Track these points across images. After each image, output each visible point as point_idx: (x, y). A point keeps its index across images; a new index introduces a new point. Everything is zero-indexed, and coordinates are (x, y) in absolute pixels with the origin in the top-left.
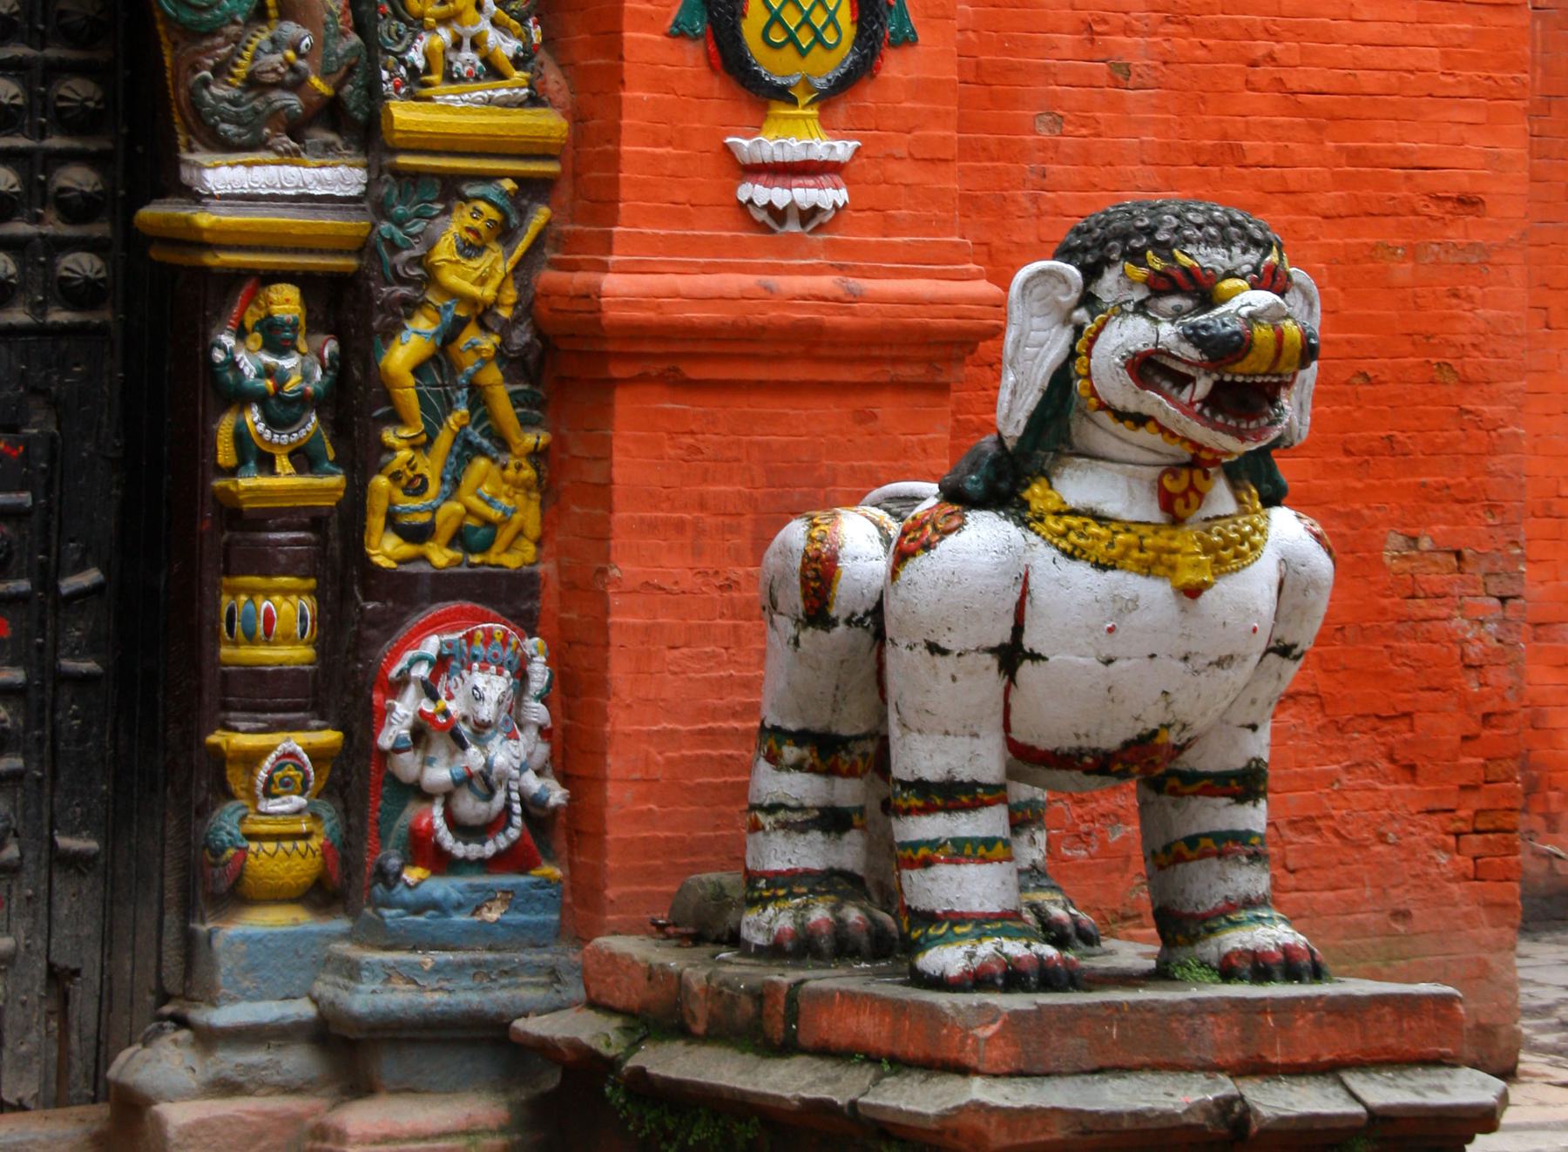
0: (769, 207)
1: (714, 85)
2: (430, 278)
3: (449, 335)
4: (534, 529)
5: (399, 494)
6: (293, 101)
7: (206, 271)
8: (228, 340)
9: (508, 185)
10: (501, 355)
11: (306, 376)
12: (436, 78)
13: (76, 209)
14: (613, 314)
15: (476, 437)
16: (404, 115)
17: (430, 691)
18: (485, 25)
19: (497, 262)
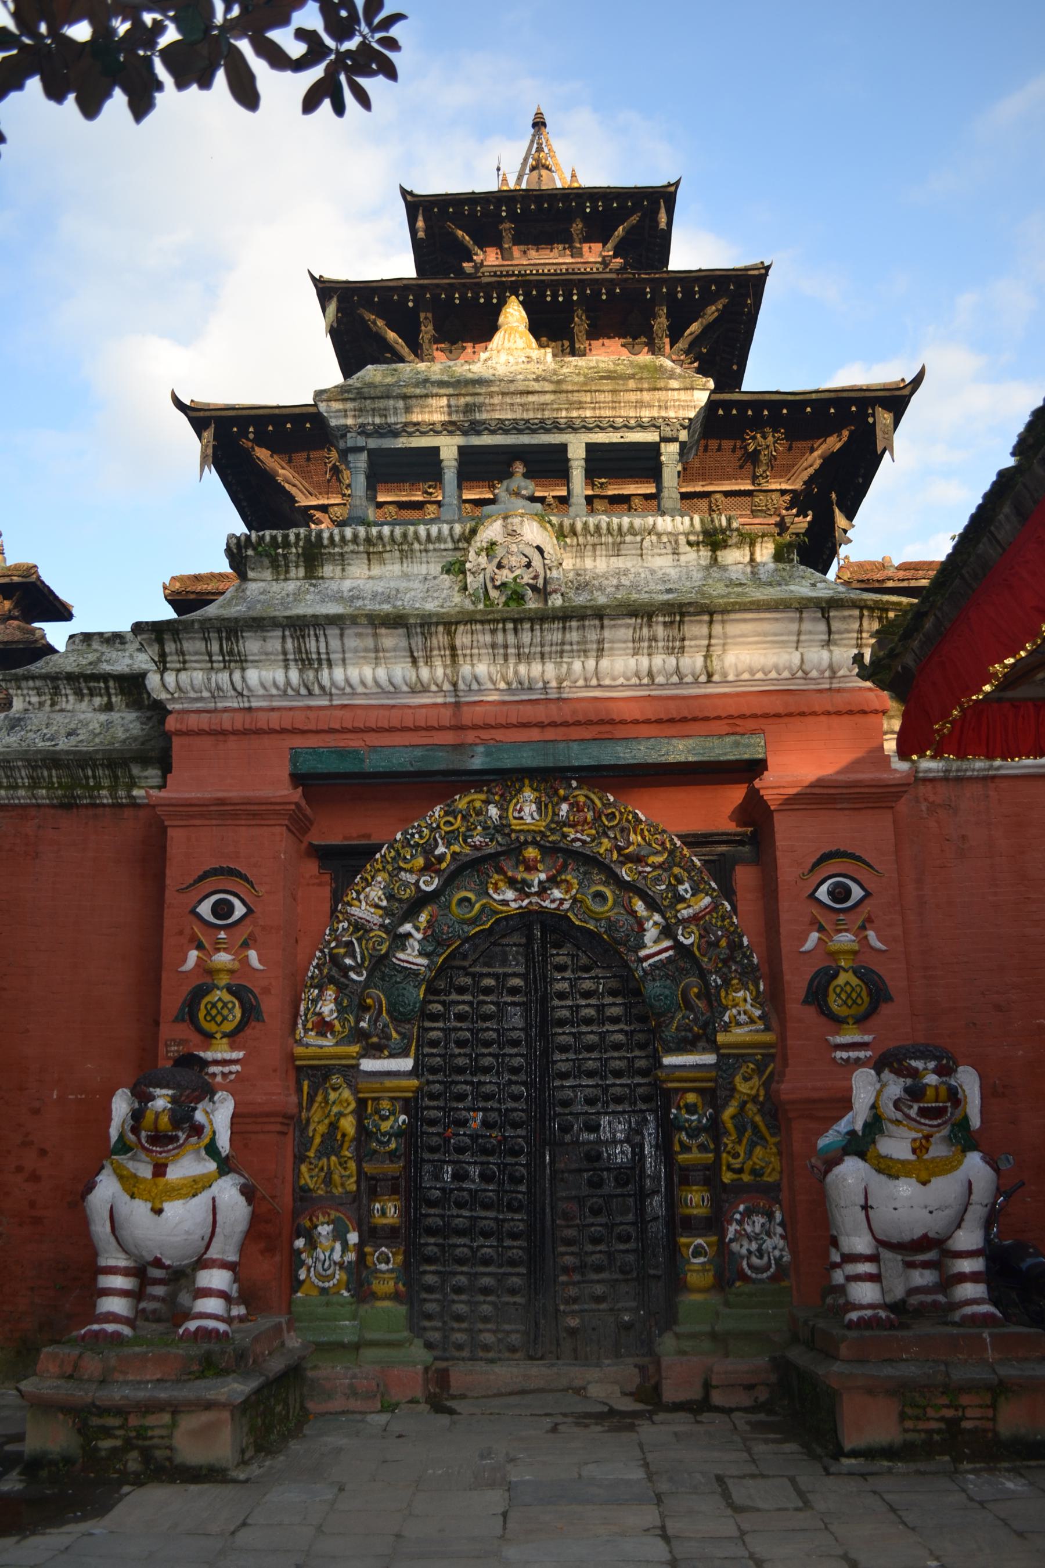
0: (841, 1058)
1: (823, 1020)
2: (734, 1089)
3: (743, 1105)
4: (779, 1169)
5: (730, 1159)
6: (689, 1035)
8: (674, 1111)
9: (759, 1057)
10: (759, 1110)
11: (699, 1121)
13: (644, 1073)
14: (783, 1097)
15: (755, 1139)
16: (721, 1038)
17: (740, 1223)
18: (748, 1007)
19: (755, 1081)
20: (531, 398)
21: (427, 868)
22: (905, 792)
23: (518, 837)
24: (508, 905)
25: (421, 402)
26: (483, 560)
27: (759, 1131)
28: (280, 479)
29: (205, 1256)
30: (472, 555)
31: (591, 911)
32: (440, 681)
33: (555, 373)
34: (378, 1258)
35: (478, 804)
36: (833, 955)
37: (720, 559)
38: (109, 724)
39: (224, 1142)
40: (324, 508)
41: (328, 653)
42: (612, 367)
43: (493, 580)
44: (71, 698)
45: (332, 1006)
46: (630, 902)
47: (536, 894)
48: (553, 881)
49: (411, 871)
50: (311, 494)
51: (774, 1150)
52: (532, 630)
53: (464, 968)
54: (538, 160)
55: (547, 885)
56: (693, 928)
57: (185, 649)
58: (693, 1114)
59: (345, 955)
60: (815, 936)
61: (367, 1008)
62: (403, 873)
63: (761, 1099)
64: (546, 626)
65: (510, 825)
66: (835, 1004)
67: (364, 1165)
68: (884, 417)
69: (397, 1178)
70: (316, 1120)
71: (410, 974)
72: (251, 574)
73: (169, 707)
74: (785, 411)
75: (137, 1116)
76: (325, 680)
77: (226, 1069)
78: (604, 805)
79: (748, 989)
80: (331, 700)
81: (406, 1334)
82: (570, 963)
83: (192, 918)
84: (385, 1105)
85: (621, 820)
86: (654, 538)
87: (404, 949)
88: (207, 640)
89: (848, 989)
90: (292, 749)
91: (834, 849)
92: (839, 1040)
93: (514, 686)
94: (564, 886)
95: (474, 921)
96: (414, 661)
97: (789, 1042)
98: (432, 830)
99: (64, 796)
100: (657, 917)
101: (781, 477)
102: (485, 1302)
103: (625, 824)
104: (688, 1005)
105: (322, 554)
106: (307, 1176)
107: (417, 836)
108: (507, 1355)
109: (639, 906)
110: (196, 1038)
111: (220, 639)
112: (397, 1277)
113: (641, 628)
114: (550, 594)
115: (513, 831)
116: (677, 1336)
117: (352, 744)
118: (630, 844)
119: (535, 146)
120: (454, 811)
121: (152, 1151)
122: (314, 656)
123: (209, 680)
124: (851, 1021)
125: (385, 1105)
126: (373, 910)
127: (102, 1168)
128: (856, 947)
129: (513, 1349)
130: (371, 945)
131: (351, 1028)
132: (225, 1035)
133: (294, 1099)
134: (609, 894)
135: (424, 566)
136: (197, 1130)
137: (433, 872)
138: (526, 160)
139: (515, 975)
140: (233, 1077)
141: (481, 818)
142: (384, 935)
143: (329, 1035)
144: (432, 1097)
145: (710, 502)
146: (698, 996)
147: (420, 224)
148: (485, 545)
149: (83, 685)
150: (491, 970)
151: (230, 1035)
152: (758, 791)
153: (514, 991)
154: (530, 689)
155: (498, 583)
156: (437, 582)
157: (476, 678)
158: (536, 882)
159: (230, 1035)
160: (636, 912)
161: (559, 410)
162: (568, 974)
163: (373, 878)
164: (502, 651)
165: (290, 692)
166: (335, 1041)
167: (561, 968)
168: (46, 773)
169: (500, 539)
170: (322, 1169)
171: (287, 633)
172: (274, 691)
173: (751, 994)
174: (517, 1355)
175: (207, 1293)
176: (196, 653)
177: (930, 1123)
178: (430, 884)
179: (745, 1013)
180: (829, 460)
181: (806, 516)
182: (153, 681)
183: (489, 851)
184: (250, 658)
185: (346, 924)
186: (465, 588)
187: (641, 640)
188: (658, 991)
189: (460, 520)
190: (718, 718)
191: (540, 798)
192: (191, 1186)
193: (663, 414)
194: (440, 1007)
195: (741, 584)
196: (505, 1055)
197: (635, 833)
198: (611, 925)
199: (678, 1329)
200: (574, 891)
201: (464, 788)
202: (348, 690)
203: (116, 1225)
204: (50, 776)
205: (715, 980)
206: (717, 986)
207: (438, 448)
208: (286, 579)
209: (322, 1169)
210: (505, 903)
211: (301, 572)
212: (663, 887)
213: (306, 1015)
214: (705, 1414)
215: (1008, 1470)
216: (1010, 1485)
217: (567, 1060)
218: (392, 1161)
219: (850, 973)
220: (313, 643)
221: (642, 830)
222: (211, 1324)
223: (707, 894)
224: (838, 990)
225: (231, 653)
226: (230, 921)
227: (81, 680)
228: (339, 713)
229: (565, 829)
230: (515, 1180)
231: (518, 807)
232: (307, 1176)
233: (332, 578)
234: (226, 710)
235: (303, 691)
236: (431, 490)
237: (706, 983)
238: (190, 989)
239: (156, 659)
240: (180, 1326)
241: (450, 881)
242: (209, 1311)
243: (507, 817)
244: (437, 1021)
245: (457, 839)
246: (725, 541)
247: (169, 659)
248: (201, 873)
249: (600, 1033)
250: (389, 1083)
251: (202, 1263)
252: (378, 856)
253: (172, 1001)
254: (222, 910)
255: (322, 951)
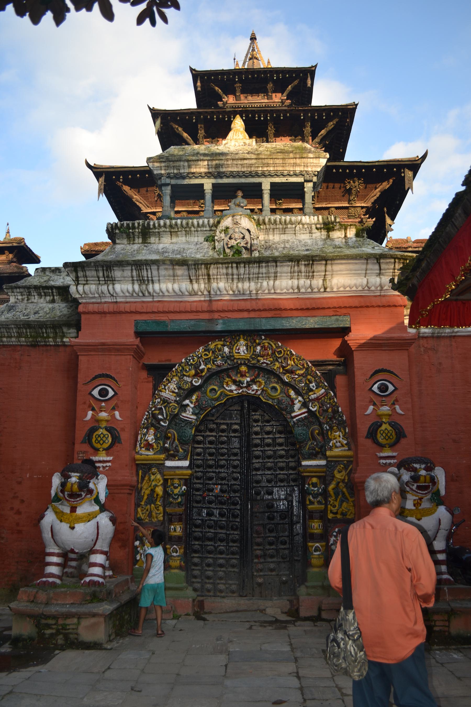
0: (383, 463)
1: (374, 445)
2: (334, 476)
4: (354, 513)
5: (332, 508)
6: (314, 451)
7: (301, 476)
8: (307, 486)
9: (346, 462)
10: (345, 486)
11: (318, 490)
12: (334, 447)
13: (294, 469)
14: (356, 480)
15: (343, 499)
16: (328, 453)
18: (341, 439)
19: (344, 473)
20: (245, 162)
21: (196, 375)
22: (414, 342)
23: (237, 362)
24: (233, 392)
25: (195, 163)
26: (223, 235)
27: (345, 496)
28: (134, 200)
29: (94, 548)
30: (218, 233)
31: (270, 395)
32: (202, 290)
33: (257, 150)
34: (172, 550)
35: (219, 346)
36: (380, 416)
37: (331, 236)
38: (53, 308)
39: (102, 497)
40: (154, 213)
41: (152, 277)
42: (282, 147)
43: (227, 244)
44: (36, 297)
45: (153, 437)
46: (288, 391)
47: (246, 387)
48: (253, 381)
49: (189, 376)
50: (148, 207)
51: (352, 504)
52: (245, 267)
53: (213, 420)
54: (252, 55)
55: (250, 383)
56: (316, 403)
57: (87, 275)
58: (315, 488)
59: (159, 414)
60: (371, 407)
61: (168, 438)
62: (185, 377)
63: (346, 481)
64: (251, 265)
65: (234, 356)
66: (380, 439)
67: (167, 508)
68: (409, 174)
69: (181, 515)
70: (145, 488)
71: (188, 423)
72: (118, 241)
73: (80, 301)
74: (364, 170)
75: (63, 485)
76: (151, 290)
77: (105, 465)
78: (276, 347)
79: (341, 431)
80: (153, 299)
81: (185, 584)
82: (260, 419)
83: (90, 397)
84: (176, 481)
85: (284, 354)
86: (301, 226)
87: (185, 411)
88: (97, 271)
89: (386, 432)
90: (135, 320)
91: (381, 368)
92: (382, 454)
93: (236, 293)
94: (258, 384)
95: (217, 399)
96: (191, 281)
97: (359, 455)
98: (199, 358)
99: (33, 341)
100: (300, 398)
101: (362, 200)
102: (220, 571)
103: (286, 356)
104: (314, 438)
105: (150, 232)
106: (140, 513)
107: (191, 360)
108: (230, 594)
109: (292, 393)
110: (91, 451)
111: (103, 270)
112: (181, 559)
113: (294, 267)
114: (253, 251)
115: (235, 358)
116: (307, 587)
117: (163, 318)
118: (288, 365)
119: (251, 48)
120: (208, 349)
121: (70, 501)
122: (146, 278)
123: (98, 289)
124: (387, 446)
125: (176, 481)
126: (171, 394)
127: (48, 508)
128: (390, 413)
129: (233, 592)
130: (170, 409)
131: (161, 447)
132: (104, 449)
133: (135, 478)
134: (278, 388)
135: (196, 238)
136: (90, 492)
137: (199, 377)
138: (247, 55)
139: (236, 424)
140: (107, 468)
141: (221, 353)
142: (176, 405)
143: (151, 450)
144: (198, 478)
145: (329, 212)
146: (318, 434)
147: (199, 84)
148: (224, 228)
149: (42, 291)
150: (225, 422)
151: (107, 449)
152: (346, 341)
153: (235, 431)
154: (244, 294)
155: (229, 246)
156: (202, 245)
157: (219, 289)
158: (245, 382)
159: (107, 449)
160: (291, 396)
161: (258, 167)
162: (260, 424)
163: (172, 379)
164: (231, 277)
165: (135, 295)
166: (154, 452)
167: (256, 421)
168: (24, 331)
169: (230, 226)
170: (147, 510)
171: (133, 268)
172: (127, 294)
173: (342, 433)
174: (235, 595)
175: (95, 565)
176: (92, 277)
177: (422, 492)
178: (197, 382)
179: (339, 442)
180: (383, 193)
181: (372, 219)
182: (73, 289)
183: (224, 368)
184: (117, 279)
185: (159, 400)
186: (215, 248)
187: (294, 272)
188: (300, 432)
189: (212, 217)
190: (329, 308)
191: (248, 343)
192: (87, 517)
193: (306, 169)
194: (202, 438)
195: (340, 247)
196: (230, 460)
197: (291, 360)
198: (279, 402)
199: (308, 584)
200: (262, 386)
201: (213, 339)
202: (161, 294)
203: (54, 534)
204: (27, 332)
205: (326, 427)
206: (327, 429)
207: (203, 184)
208: (133, 244)
209: (147, 510)
210: (231, 391)
211: (140, 240)
212: (303, 385)
213: (141, 441)
214: (318, 622)
215: (455, 649)
216: (455, 656)
217: (259, 462)
218: (179, 507)
219: (387, 424)
220: (145, 272)
221: (294, 359)
222: (96, 579)
223: (323, 388)
224: (382, 432)
225: (108, 277)
226: (107, 398)
227: (41, 289)
228: (157, 304)
229: (259, 358)
230: (235, 516)
231: (238, 348)
232: (140, 513)
233: (154, 243)
234: (106, 303)
235: (141, 294)
236: (202, 205)
237: (322, 428)
238: (88, 428)
239: (74, 279)
240: (82, 580)
241: (206, 381)
242: (95, 573)
243: (233, 352)
244: (200, 444)
245: (210, 362)
246: (333, 227)
247: (80, 279)
248: (94, 376)
249: (274, 450)
250: (178, 472)
251: (92, 551)
252: (174, 369)
253: (80, 434)
254: (103, 393)
255: (148, 412)
